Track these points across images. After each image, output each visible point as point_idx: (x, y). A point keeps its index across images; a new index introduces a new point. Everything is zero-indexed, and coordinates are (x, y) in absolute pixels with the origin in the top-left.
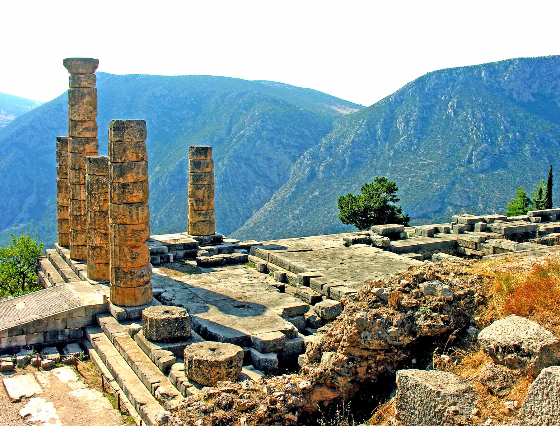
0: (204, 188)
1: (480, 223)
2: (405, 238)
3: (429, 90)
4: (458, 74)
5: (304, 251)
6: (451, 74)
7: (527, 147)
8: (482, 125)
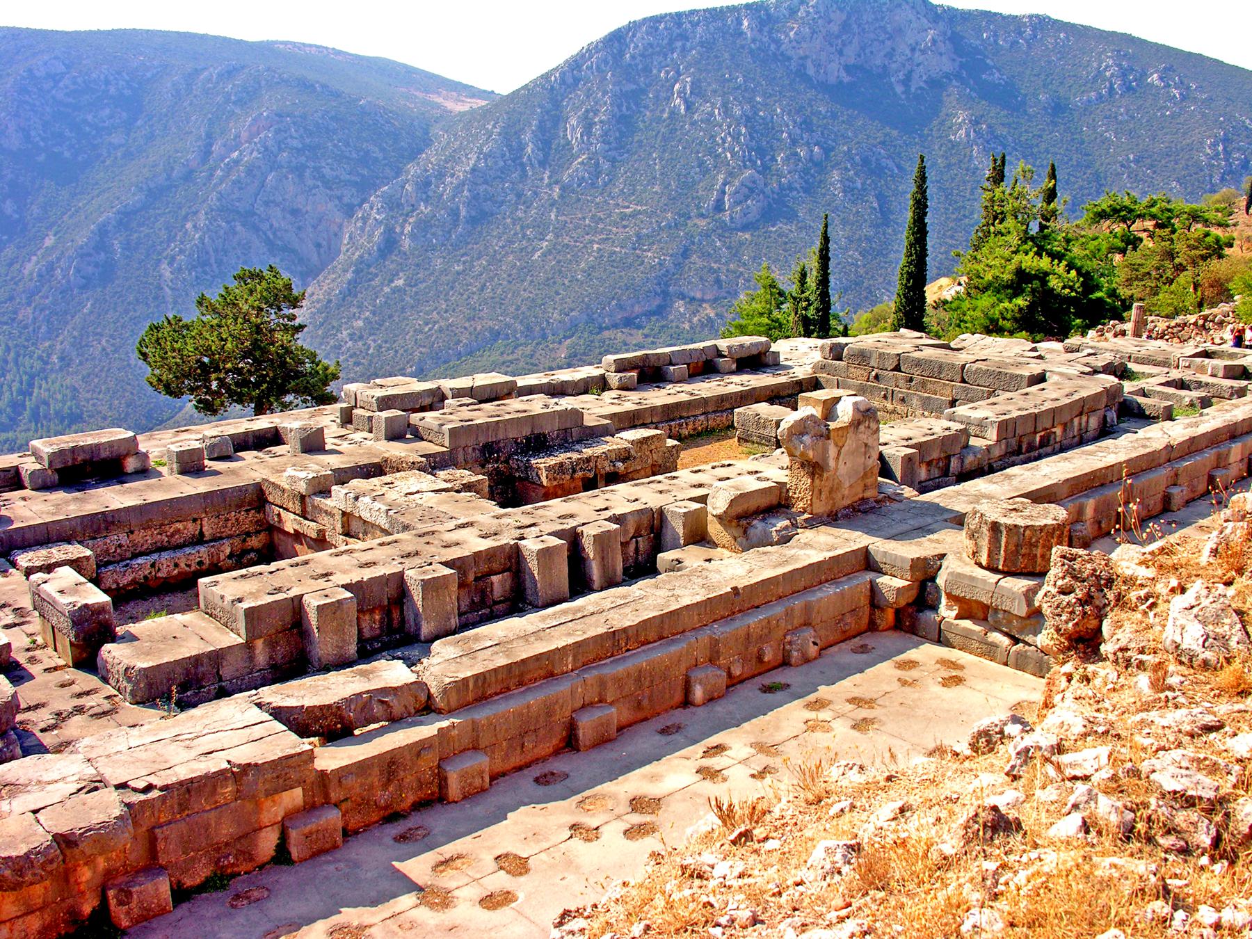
2: (144, 472)
3: (633, 57)
4: (695, 25)
6: (679, 25)
7: (836, 175)
8: (743, 130)
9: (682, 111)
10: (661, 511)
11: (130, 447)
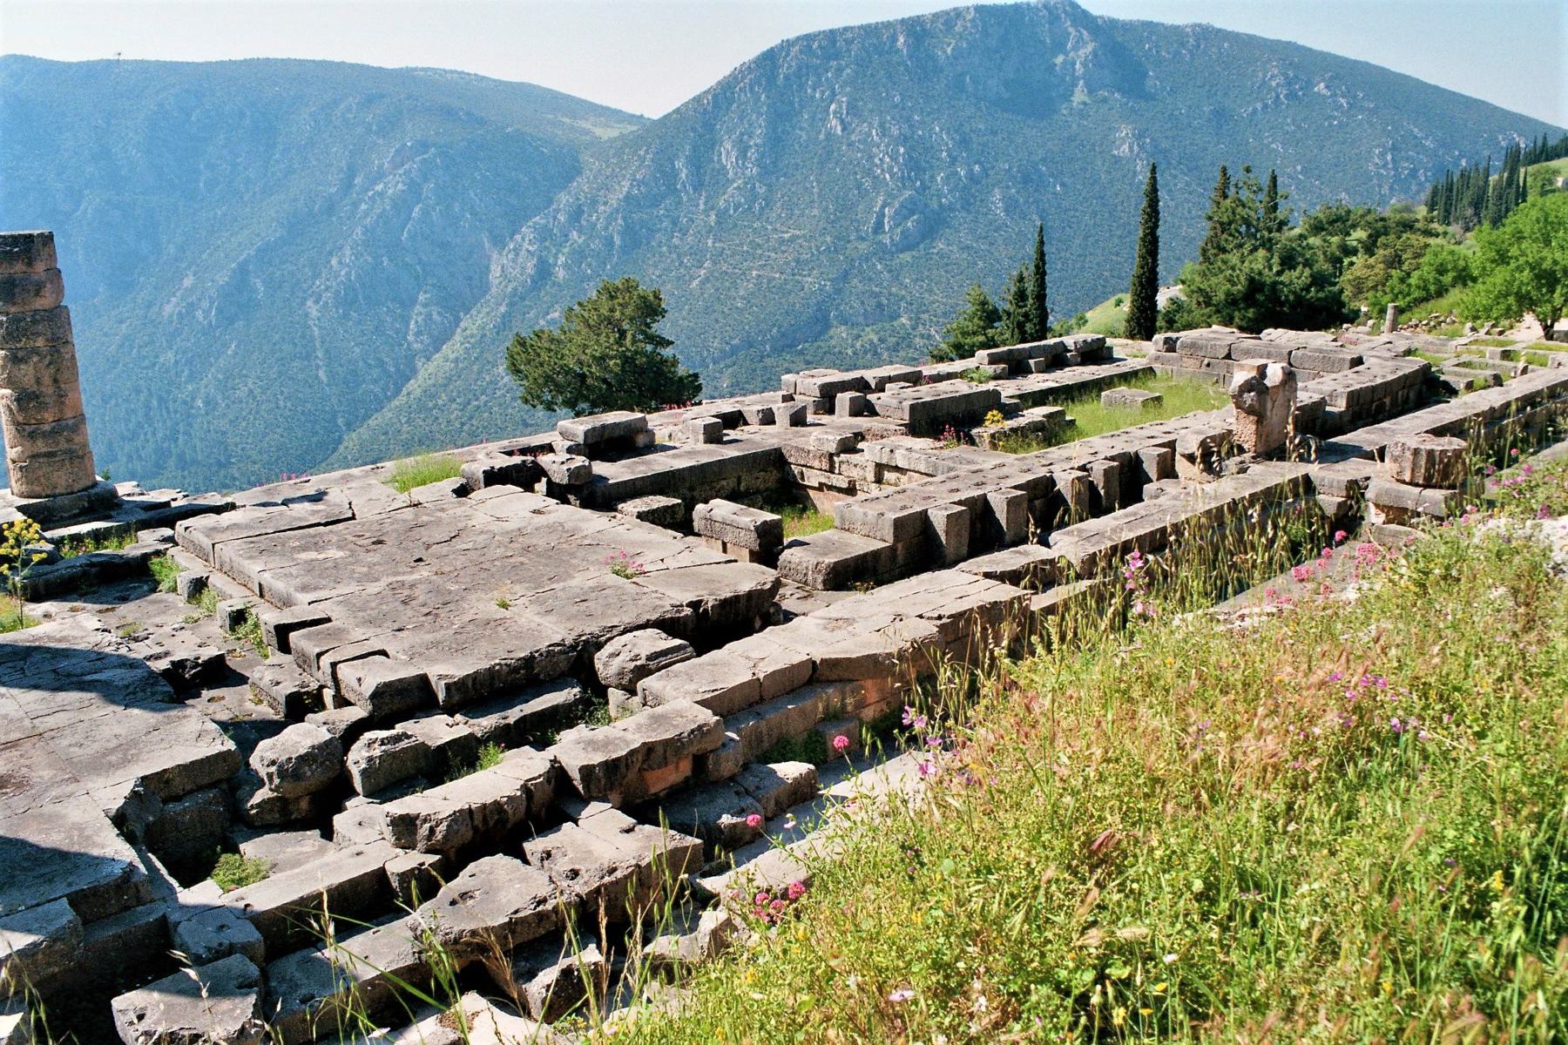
0: (35, 359)
1: (848, 395)
2: (651, 448)
3: (787, 78)
4: (849, 42)
5: (326, 524)
6: (834, 42)
7: (997, 195)
8: (902, 150)
9: (839, 132)
10: (1136, 454)
11: (641, 428)
